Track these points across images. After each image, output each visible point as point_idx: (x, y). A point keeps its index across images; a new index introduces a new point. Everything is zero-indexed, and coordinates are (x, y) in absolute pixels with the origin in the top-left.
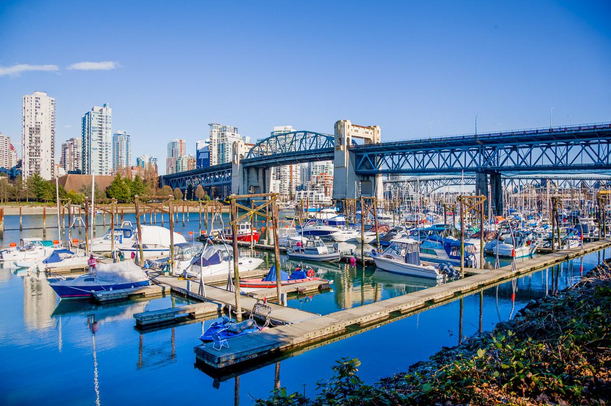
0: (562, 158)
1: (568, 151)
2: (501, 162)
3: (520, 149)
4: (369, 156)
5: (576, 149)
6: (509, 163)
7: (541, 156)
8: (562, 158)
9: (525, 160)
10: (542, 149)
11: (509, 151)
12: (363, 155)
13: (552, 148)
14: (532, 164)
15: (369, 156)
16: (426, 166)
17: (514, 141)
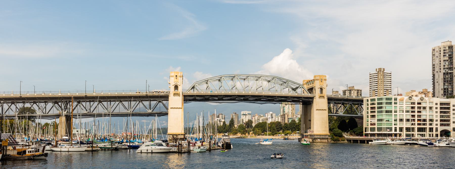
2: (92, 109)
5: (50, 105)
9: (43, 111)
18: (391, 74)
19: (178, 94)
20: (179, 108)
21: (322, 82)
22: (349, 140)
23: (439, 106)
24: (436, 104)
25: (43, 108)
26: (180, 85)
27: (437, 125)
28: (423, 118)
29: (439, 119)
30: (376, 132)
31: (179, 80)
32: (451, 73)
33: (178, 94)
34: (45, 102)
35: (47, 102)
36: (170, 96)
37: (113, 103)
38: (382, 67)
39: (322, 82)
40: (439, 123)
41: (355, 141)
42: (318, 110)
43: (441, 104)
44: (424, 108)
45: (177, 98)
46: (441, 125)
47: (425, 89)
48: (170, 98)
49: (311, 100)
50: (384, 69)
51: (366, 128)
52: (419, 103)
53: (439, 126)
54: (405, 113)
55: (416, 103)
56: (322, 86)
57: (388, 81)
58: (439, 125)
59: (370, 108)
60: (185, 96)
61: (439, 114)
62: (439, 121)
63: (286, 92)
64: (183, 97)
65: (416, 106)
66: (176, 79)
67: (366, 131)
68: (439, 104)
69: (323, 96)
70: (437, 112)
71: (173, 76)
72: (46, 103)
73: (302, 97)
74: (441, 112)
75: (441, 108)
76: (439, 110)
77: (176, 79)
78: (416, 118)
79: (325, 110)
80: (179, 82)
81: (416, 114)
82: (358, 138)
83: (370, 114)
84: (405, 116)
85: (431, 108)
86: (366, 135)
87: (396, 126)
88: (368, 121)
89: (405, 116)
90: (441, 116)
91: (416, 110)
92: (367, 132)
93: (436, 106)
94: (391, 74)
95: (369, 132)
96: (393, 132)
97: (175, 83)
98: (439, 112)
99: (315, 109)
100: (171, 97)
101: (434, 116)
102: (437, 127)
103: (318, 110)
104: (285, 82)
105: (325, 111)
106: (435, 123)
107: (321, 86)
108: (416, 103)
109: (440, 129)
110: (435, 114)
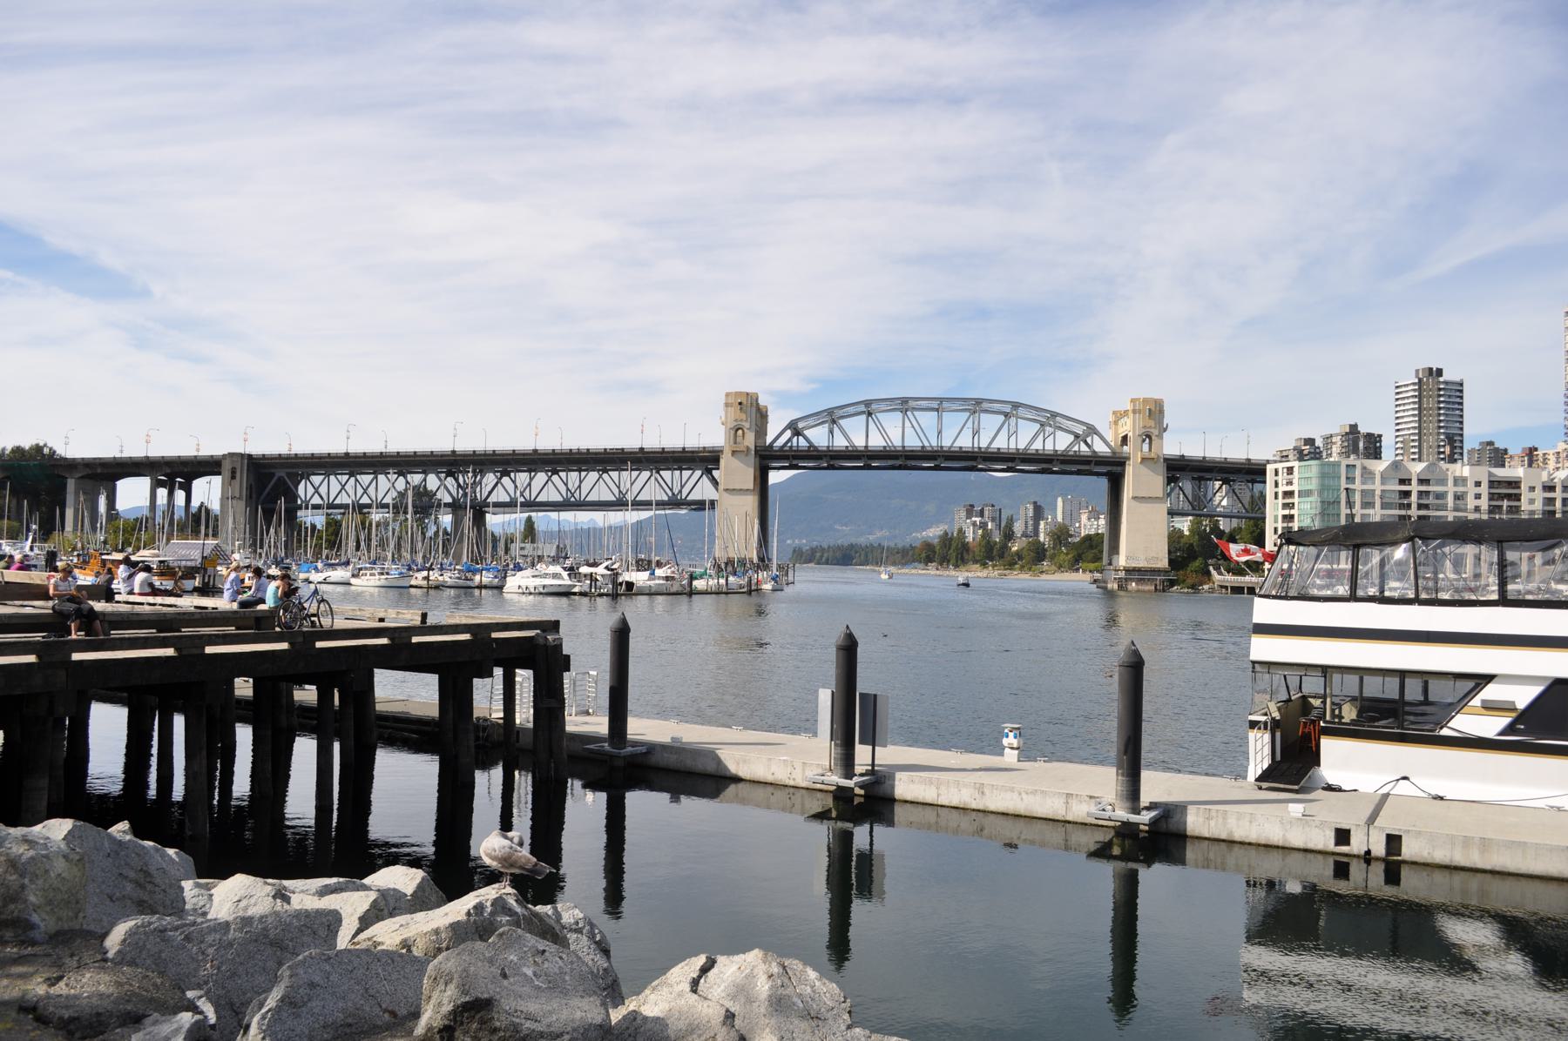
0: (575, 491)
1: (531, 479)
3: (409, 475)
4: (289, 475)
5: (541, 477)
6: (500, 496)
7: (545, 485)
8: (575, 491)
10: (547, 475)
11: (443, 475)
12: (273, 474)
13: (561, 474)
14: (532, 499)
15: (289, 475)
16: (310, 499)
17: (506, 463)
23: (1484, 490)
24: (1478, 484)
25: (525, 486)
34: (530, 471)
35: (534, 471)
37: (686, 474)
44: (1441, 496)
48: (722, 462)
49: (1119, 469)
55: (1414, 482)
57: (1408, 410)
64: (758, 459)
68: (1485, 485)
72: (533, 474)
82: (1245, 582)
93: (1478, 490)
104: (1050, 420)
108: (1414, 482)
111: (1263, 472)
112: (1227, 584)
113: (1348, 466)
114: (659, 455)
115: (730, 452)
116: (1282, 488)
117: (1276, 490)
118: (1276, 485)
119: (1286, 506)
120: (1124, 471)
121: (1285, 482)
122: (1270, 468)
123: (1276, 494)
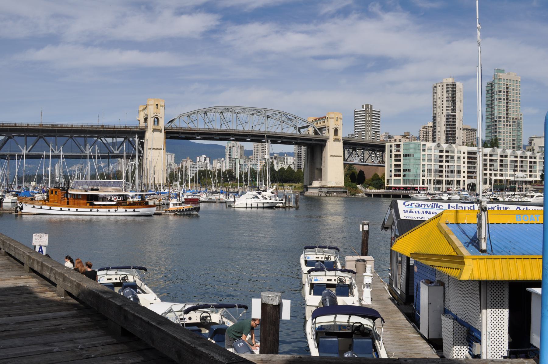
18: (379, 112)
19: (159, 130)
20: (156, 149)
21: (337, 121)
22: (369, 195)
23: (466, 155)
24: (464, 153)
26: (161, 118)
27: (464, 177)
28: (451, 169)
29: (466, 170)
30: (402, 185)
31: (161, 111)
32: (453, 116)
33: (159, 129)
36: (147, 132)
38: (370, 104)
39: (337, 121)
40: (466, 175)
41: (378, 196)
42: (332, 156)
43: (469, 153)
44: (453, 157)
45: (157, 134)
46: (469, 177)
47: (407, 132)
49: (323, 143)
50: (371, 106)
51: (388, 180)
52: (447, 152)
53: (466, 179)
54: (433, 163)
55: (444, 152)
56: (338, 126)
58: (466, 177)
59: (393, 156)
60: (167, 133)
61: (466, 165)
62: (466, 172)
63: (290, 131)
65: (444, 154)
66: (157, 108)
67: (387, 184)
68: (466, 153)
69: (339, 139)
70: (464, 163)
71: (151, 105)
73: (283, 137)
74: (468, 162)
75: (469, 158)
76: (466, 160)
77: (157, 108)
78: (444, 169)
79: (340, 156)
80: (161, 113)
81: (444, 164)
83: (394, 163)
84: (433, 166)
85: (459, 158)
86: (390, 188)
87: (423, 178)
88: (391, 171)
89: (433, 166)
90: (469, 167)
91: (444, 159)
92: (389, 185)
94: (379, 112)
95: (392, 185)
96: (421, 185)
97: (155, 114)
98: (466, 163)
99: (329, 155)
100: (149, 135)
101: (462, 167)
102: (464, 179)
103: (332, 156)
104: (290, 119)
105: (340, 157)
106: (462, 174)
107: (336, 126)
108: (444, 152)
109: (467, 181)
110: (462, 164)
111: (384, 147)
112: (372, 193)
113: (423, 144)
114: (113, 129)
115: (152, 130)
116: (394, 153)
117: (391, 154)
118: (391, 151)
119: (396, 160)
120: (325, 145)
121: (395, 150)
122: (387, 145)
123: (391, 156)
